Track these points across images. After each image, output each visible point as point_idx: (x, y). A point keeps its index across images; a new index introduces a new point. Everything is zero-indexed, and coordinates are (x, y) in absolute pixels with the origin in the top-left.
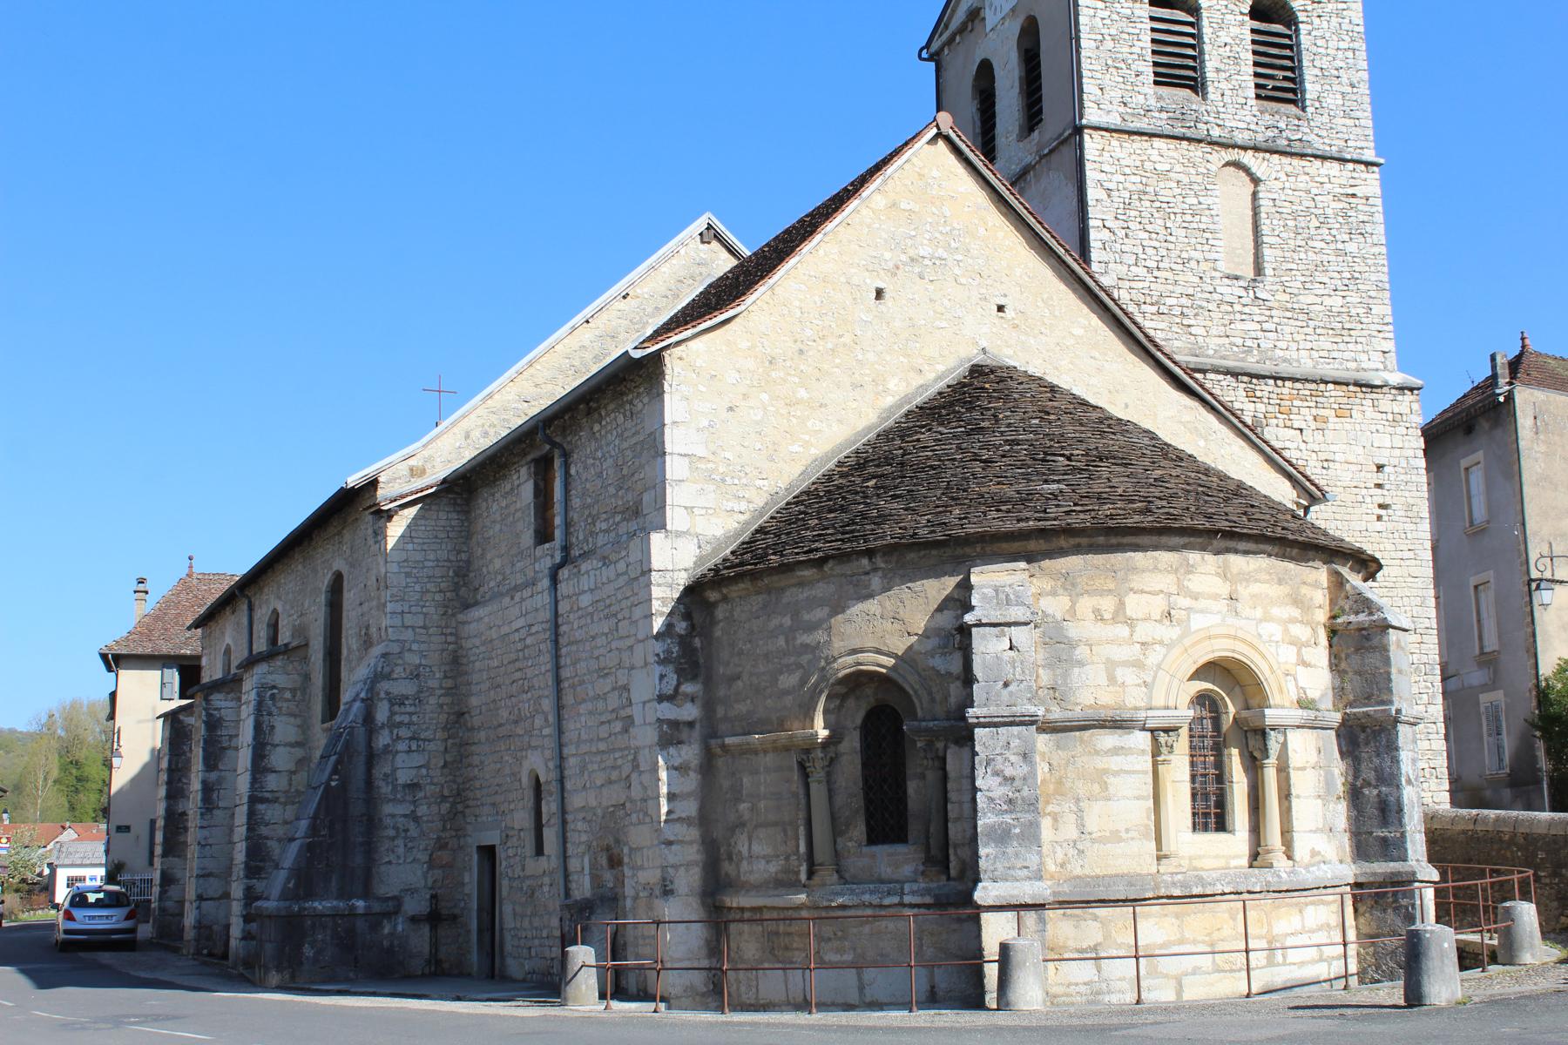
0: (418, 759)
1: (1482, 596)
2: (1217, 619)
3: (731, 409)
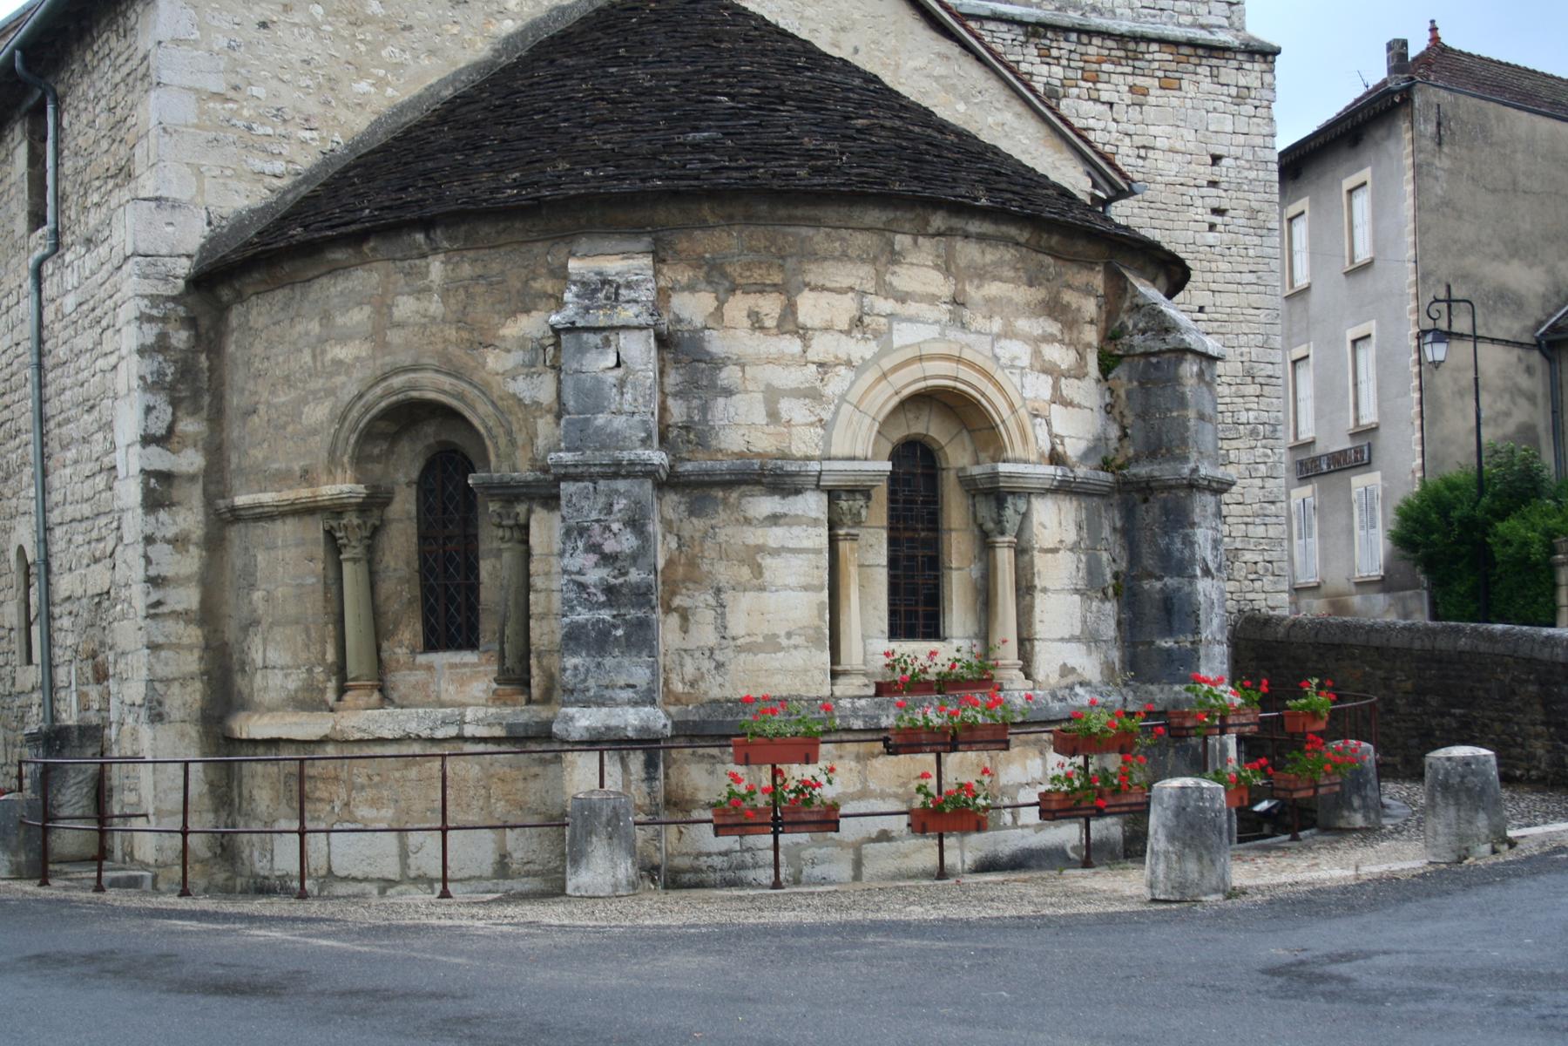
1: (1361, 354)
2: (934, 331)
3: (263, 25)
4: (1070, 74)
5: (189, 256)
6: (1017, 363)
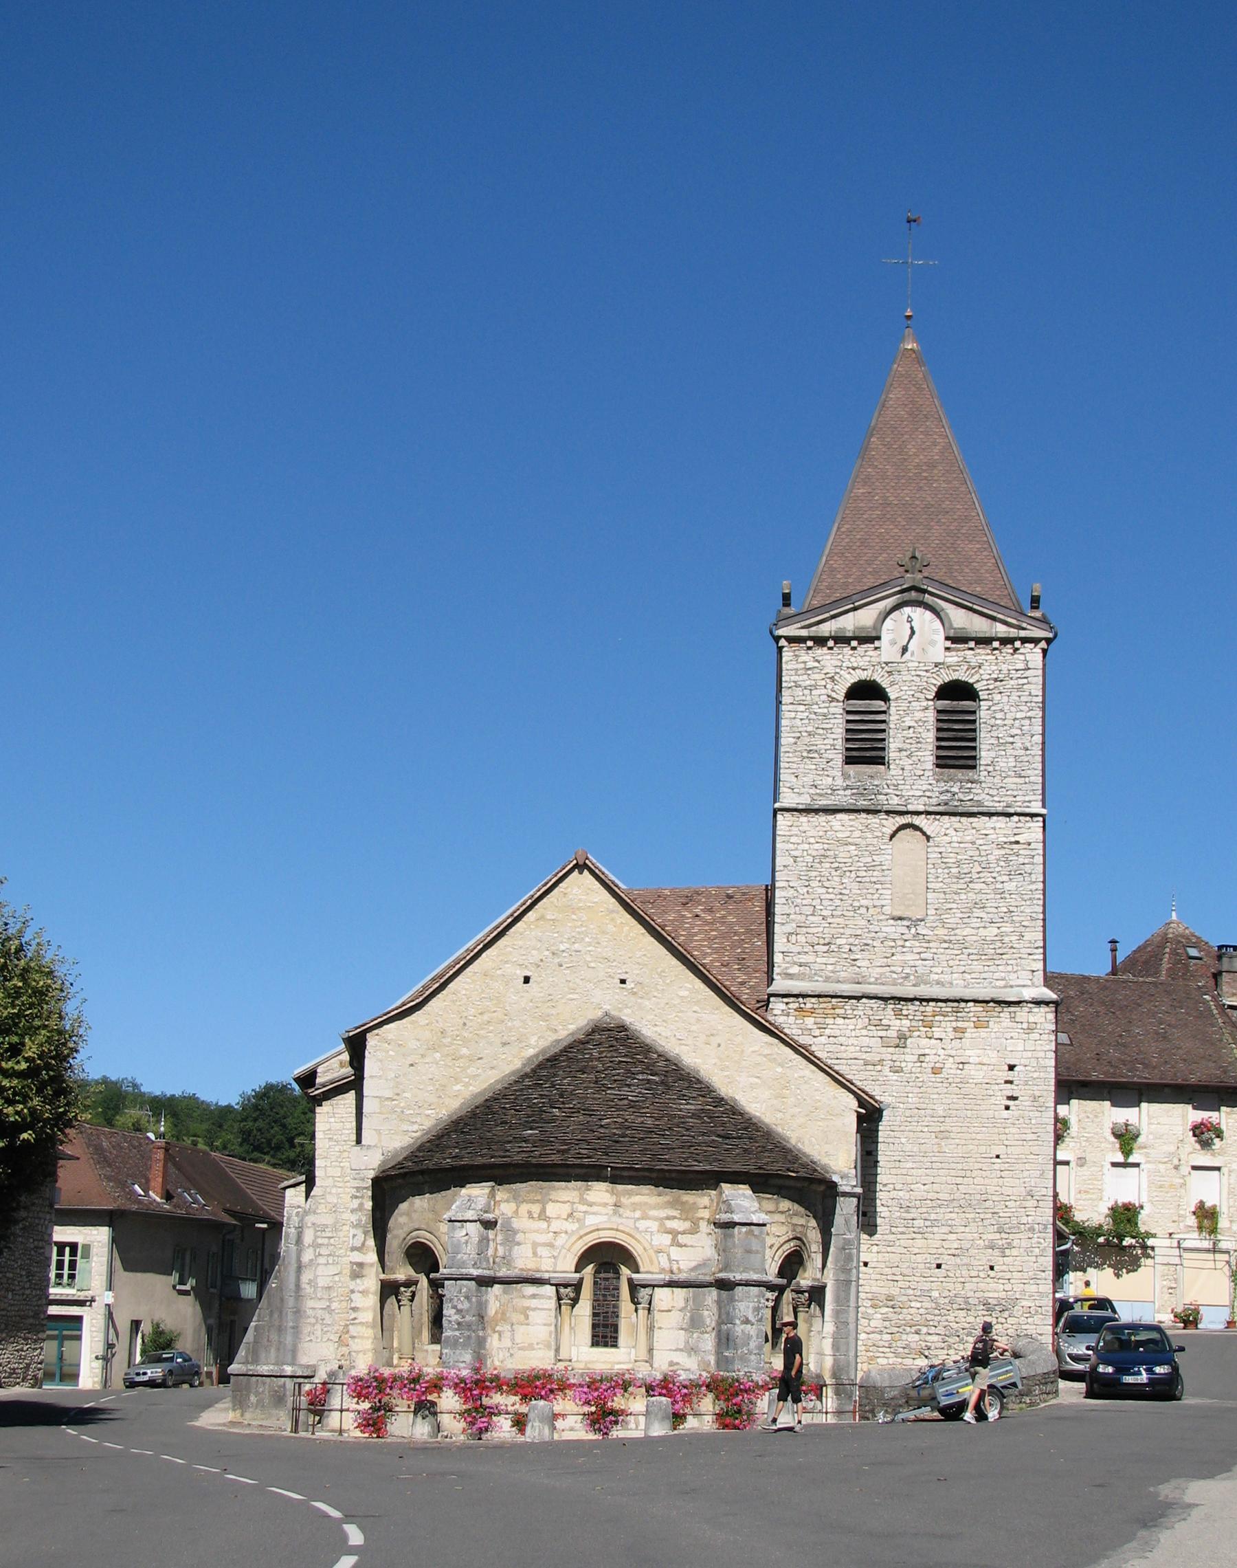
0: (333, 1270)
2: (604, 1218)
3: (412, 1065)
4: (914, 1023)
5: (374, 1169)
6: (649, 1230)
